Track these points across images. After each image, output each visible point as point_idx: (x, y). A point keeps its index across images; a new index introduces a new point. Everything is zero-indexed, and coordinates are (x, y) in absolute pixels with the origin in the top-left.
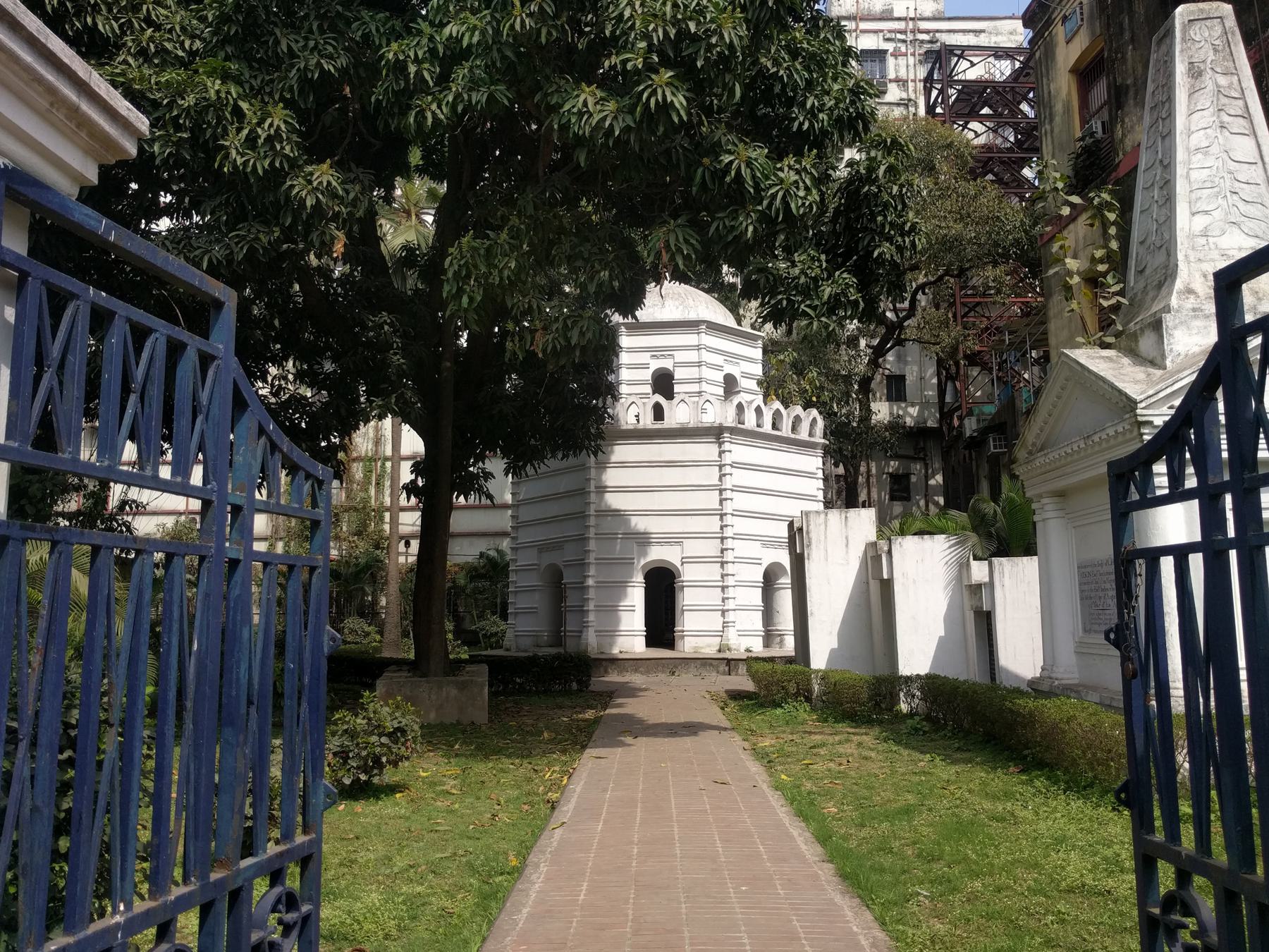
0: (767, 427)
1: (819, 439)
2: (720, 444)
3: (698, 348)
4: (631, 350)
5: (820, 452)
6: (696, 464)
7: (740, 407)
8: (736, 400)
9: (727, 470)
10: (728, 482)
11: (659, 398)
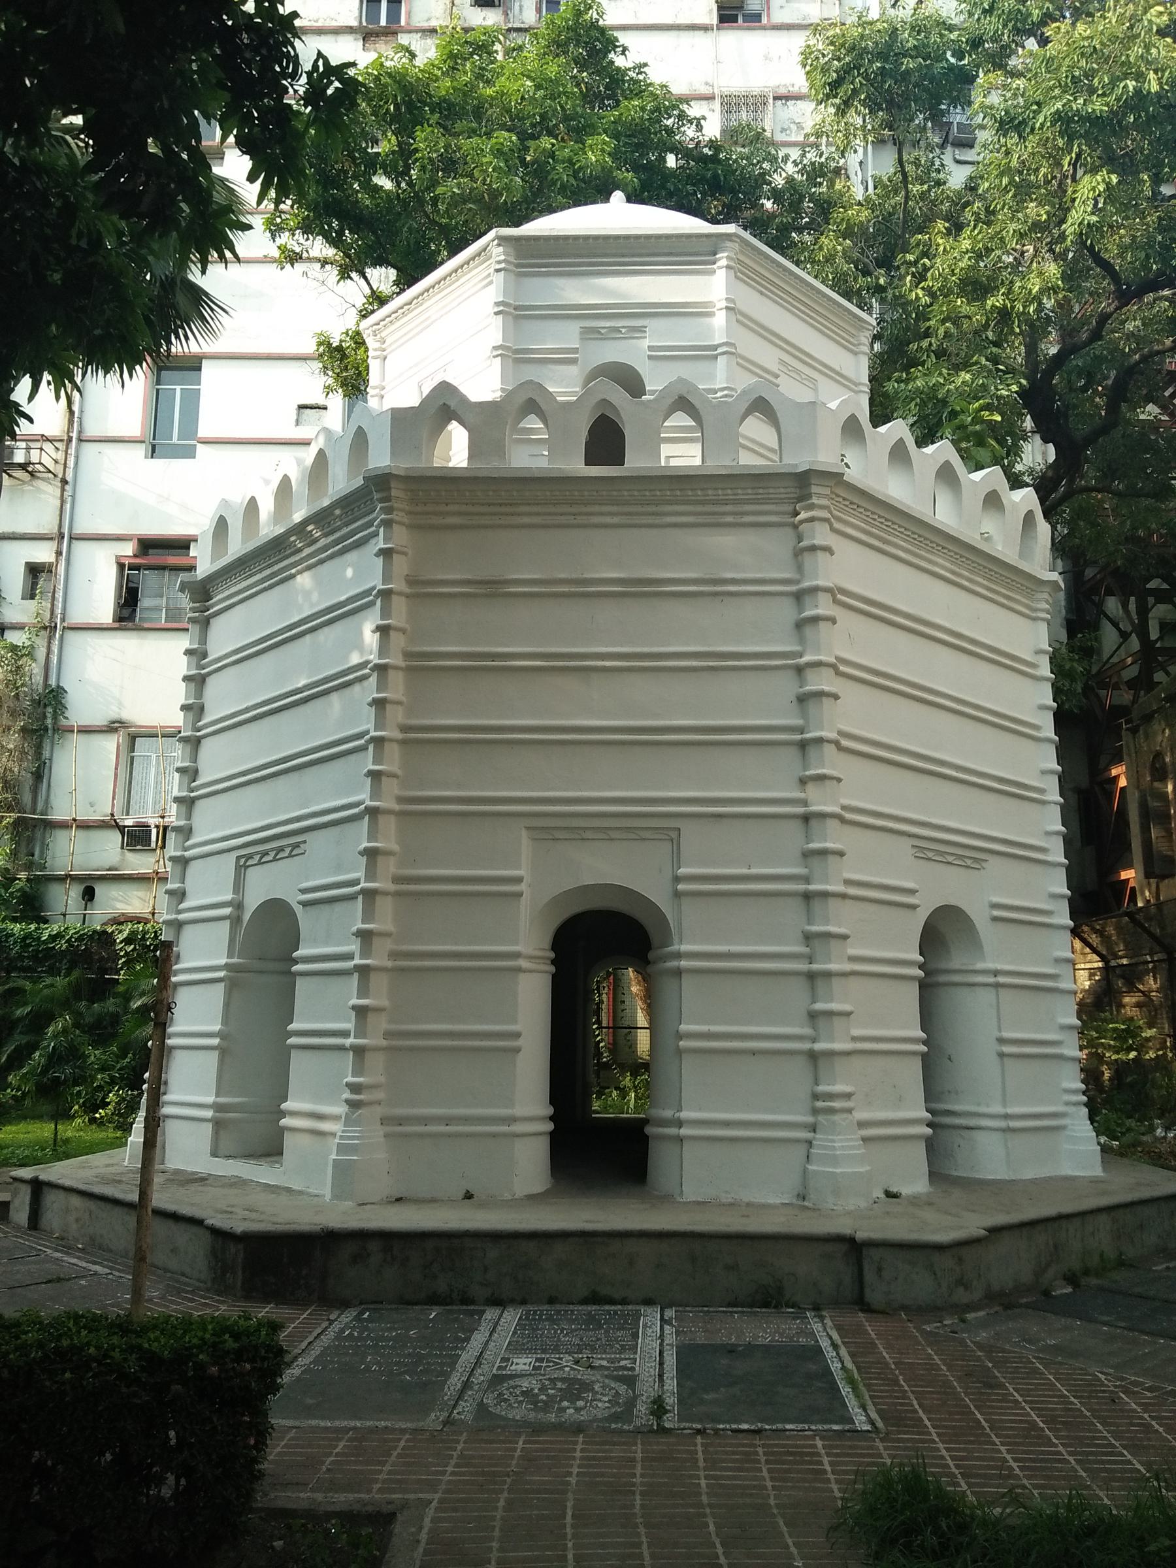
5: (1043, 603)
9: (823, 607)
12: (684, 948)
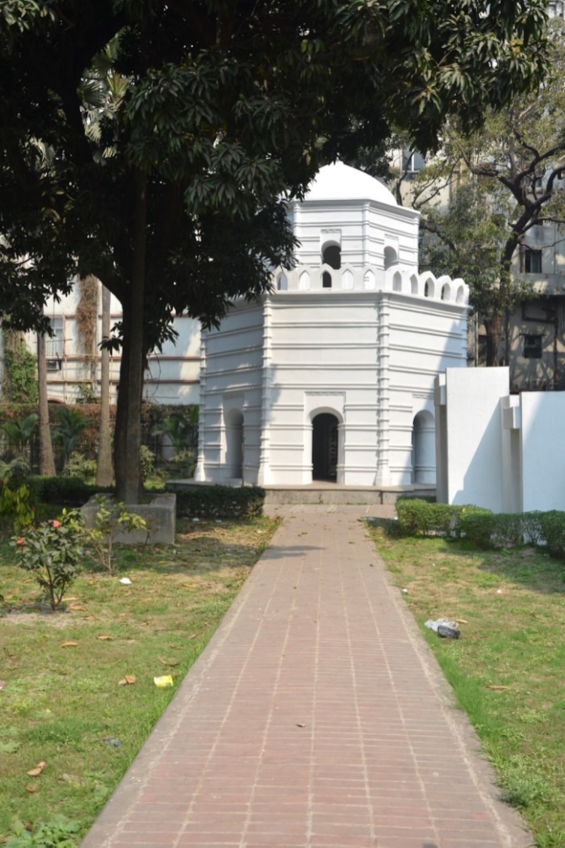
0: (420, 295)
1: (464, 304)
2: (380, 308)
3: (363, 224)
4: (305, 225)
6: (358, 326)
7: (397, 277)
8: (393, 269)
10: (386, 342)
11: (328, 268)
12: (347, 423)
